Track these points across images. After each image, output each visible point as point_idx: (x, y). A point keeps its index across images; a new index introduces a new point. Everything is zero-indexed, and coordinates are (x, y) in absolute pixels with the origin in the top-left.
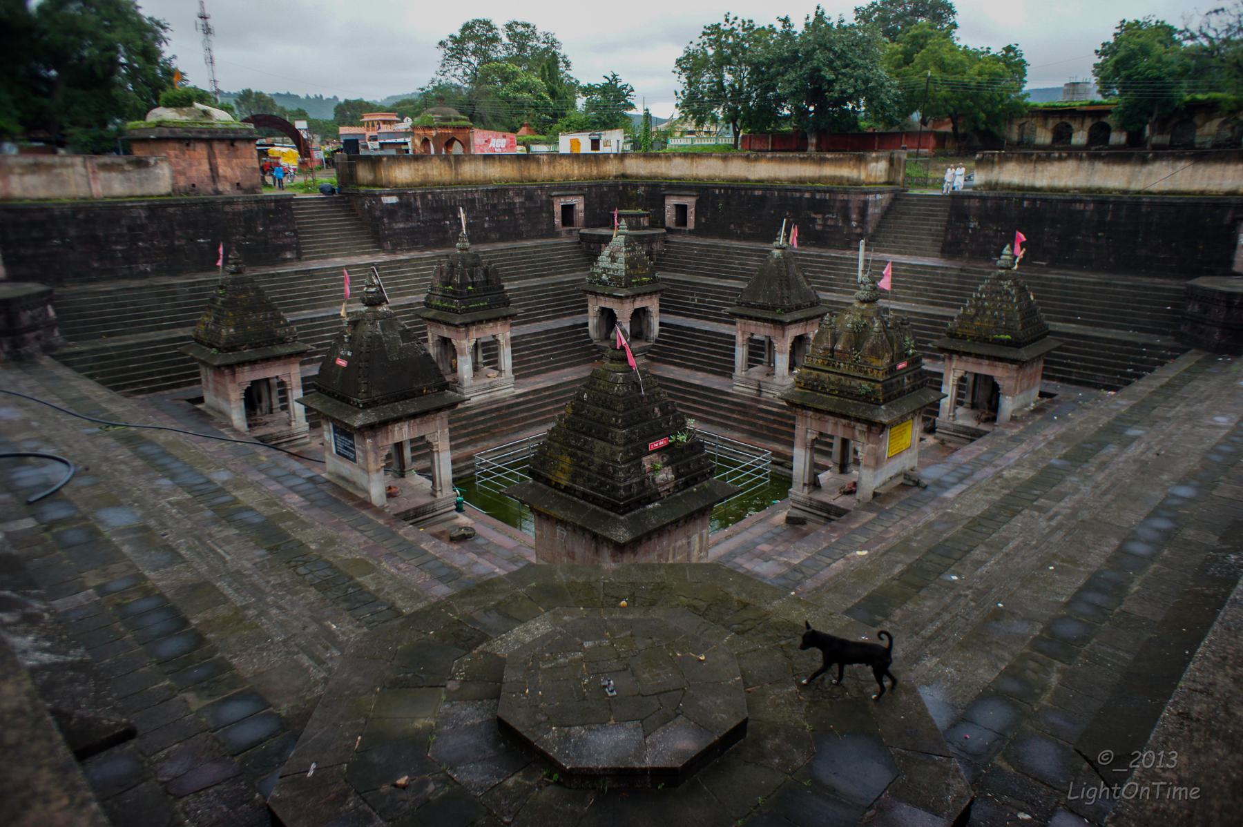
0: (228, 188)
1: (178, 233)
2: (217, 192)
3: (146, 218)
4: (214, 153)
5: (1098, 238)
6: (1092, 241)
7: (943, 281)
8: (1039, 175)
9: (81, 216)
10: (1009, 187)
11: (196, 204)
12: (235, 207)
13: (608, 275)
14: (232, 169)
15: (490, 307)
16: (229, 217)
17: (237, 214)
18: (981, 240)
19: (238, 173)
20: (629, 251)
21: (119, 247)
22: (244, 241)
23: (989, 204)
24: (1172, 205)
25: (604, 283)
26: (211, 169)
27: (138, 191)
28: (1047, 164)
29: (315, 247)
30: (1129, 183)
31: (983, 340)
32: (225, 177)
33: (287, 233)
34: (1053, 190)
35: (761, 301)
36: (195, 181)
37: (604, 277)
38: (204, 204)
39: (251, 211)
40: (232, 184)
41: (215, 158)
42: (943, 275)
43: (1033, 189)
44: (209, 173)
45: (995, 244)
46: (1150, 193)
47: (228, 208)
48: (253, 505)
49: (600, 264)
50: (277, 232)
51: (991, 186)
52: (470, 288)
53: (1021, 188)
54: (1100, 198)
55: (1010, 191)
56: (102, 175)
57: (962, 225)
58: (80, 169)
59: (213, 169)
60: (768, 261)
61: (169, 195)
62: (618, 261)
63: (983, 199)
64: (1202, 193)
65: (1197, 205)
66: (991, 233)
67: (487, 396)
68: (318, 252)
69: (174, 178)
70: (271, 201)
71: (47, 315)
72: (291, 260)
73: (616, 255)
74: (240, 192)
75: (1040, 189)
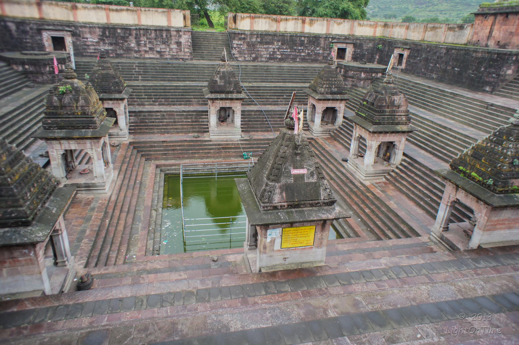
0: (493, 44)
1: (450, 63)
2: (487, 46)
3: (445, 54)
4: (495, 22)
9: (428, 49)
11: (462, 50)
12: (477, 54)
14: (500, 32)
15: (365, 118)
16: (473, 59)
17: (476, 58)
19: (501, 35)
20: (491, 141)
21: (431, 65)
22: (472, 74)
26: (490, 32)
27: (455, 42)
29: (512, 90)
32: (494, 37)
33: (494, 75)
36: (480, 39)
38: (465, 50)
39: (483, 58)
40: (495, 42)
41: (494, 25)
44: (488, 35)
47: (474, 55)
50: (490, 73)
52: (365, 103)
56: (448, 32)
58: (443, 30)
59: (491, 32)
61: (464, 44)
67: (355, 170)
68: (508, 93)
69: (473, 36)
70: (495, 54)
71: (360, 76)
72: (487, 92)
74: (497, 47)
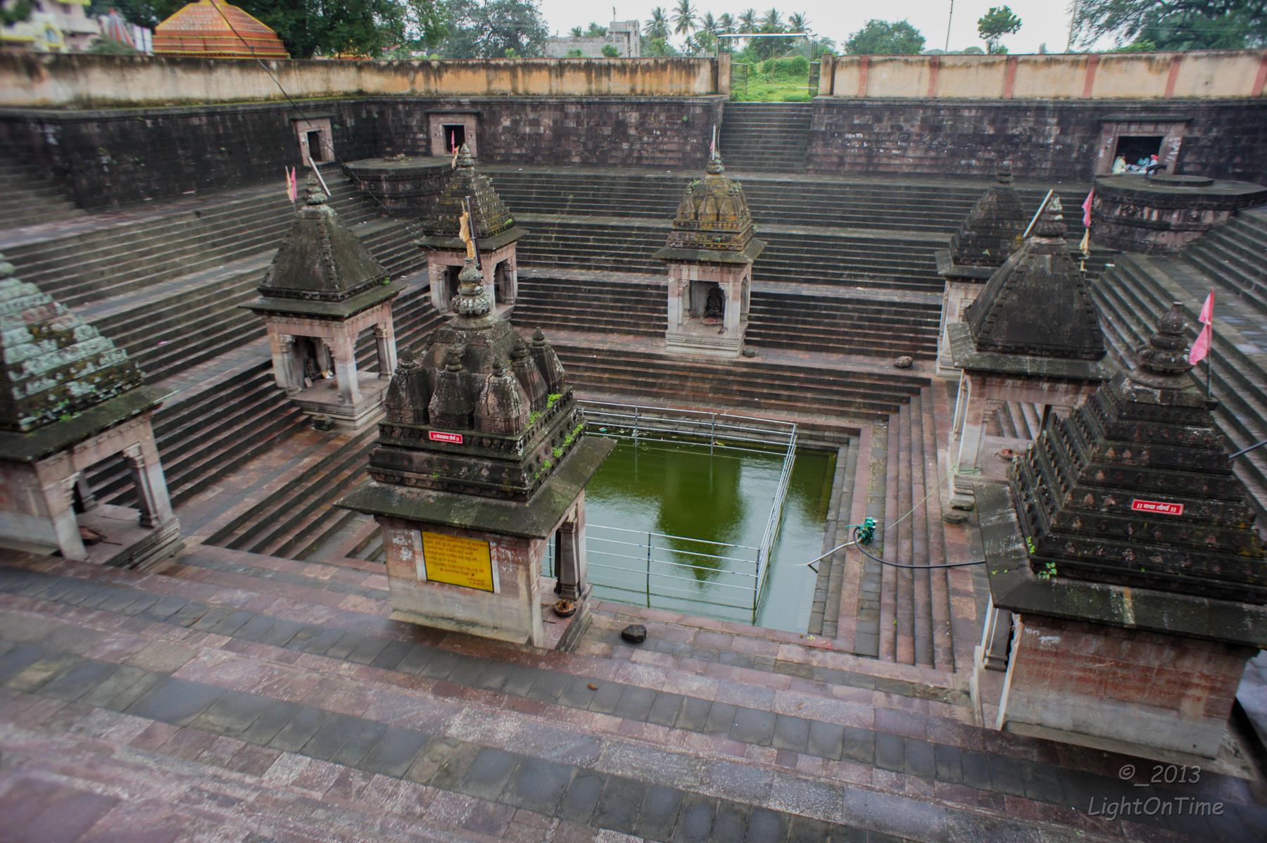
5: (221, 152)
6: (219, 157)
7: (198, 232)
8: (130, 85)
10: (104, 103)
13: (89, 379)
18: (123, 178)
23: (111, 127)
24: (256, 111)
25: (87, 402)
28: (134, 71)
30: (207, 92)
31: (503, 229)
34: (150, 103)
35: (364, 280)
37: (76, 389)
42: (188, 225)
43: (130, 104)
45: (141, 181)
46: (223, 102)
48: (1225, 325)
49: (29, 367)
51: (86, 103)
53: (118, 104)
54: (217, 113)
55: (116, 110)
57: (93, 163)
60: (328, 224)
62: (78, 335)
63: (102, 121)
64: (253, 99)
65: (268, 111)
66: (131, 168)
73: (57, 327)
75: (136, 104)
